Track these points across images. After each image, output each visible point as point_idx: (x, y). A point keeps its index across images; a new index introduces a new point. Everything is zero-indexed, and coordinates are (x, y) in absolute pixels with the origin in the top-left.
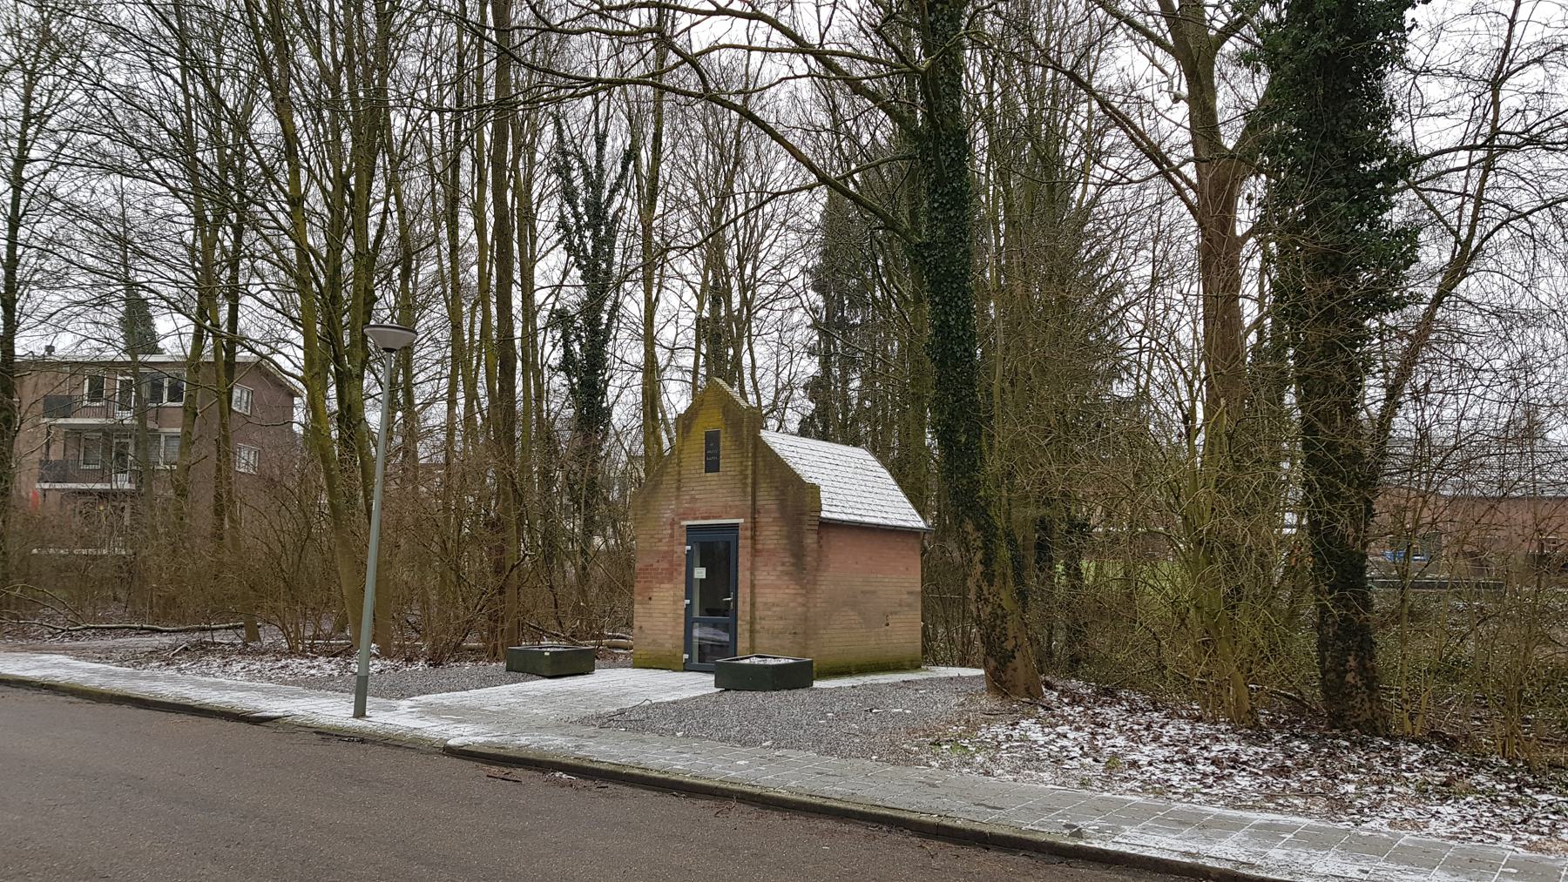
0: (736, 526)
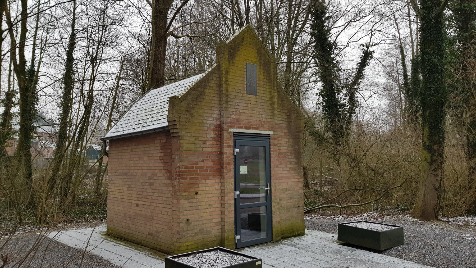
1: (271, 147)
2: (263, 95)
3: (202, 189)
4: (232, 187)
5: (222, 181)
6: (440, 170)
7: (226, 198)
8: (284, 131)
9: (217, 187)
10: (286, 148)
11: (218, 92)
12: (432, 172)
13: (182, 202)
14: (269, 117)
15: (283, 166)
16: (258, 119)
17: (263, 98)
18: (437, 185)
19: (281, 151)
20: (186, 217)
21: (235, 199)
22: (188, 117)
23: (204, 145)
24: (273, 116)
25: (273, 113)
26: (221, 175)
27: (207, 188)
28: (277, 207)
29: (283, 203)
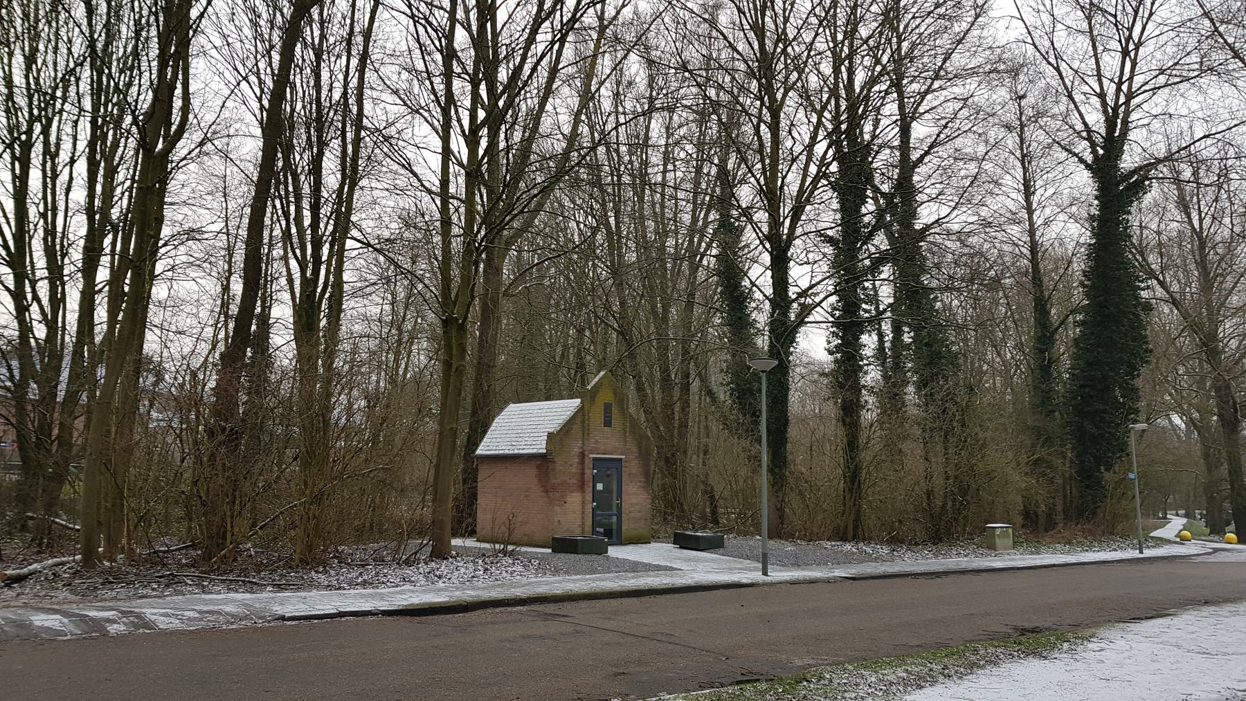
0: (621, 459)
3: (568, 500)
9: (580, 499)
18: (779, 506)
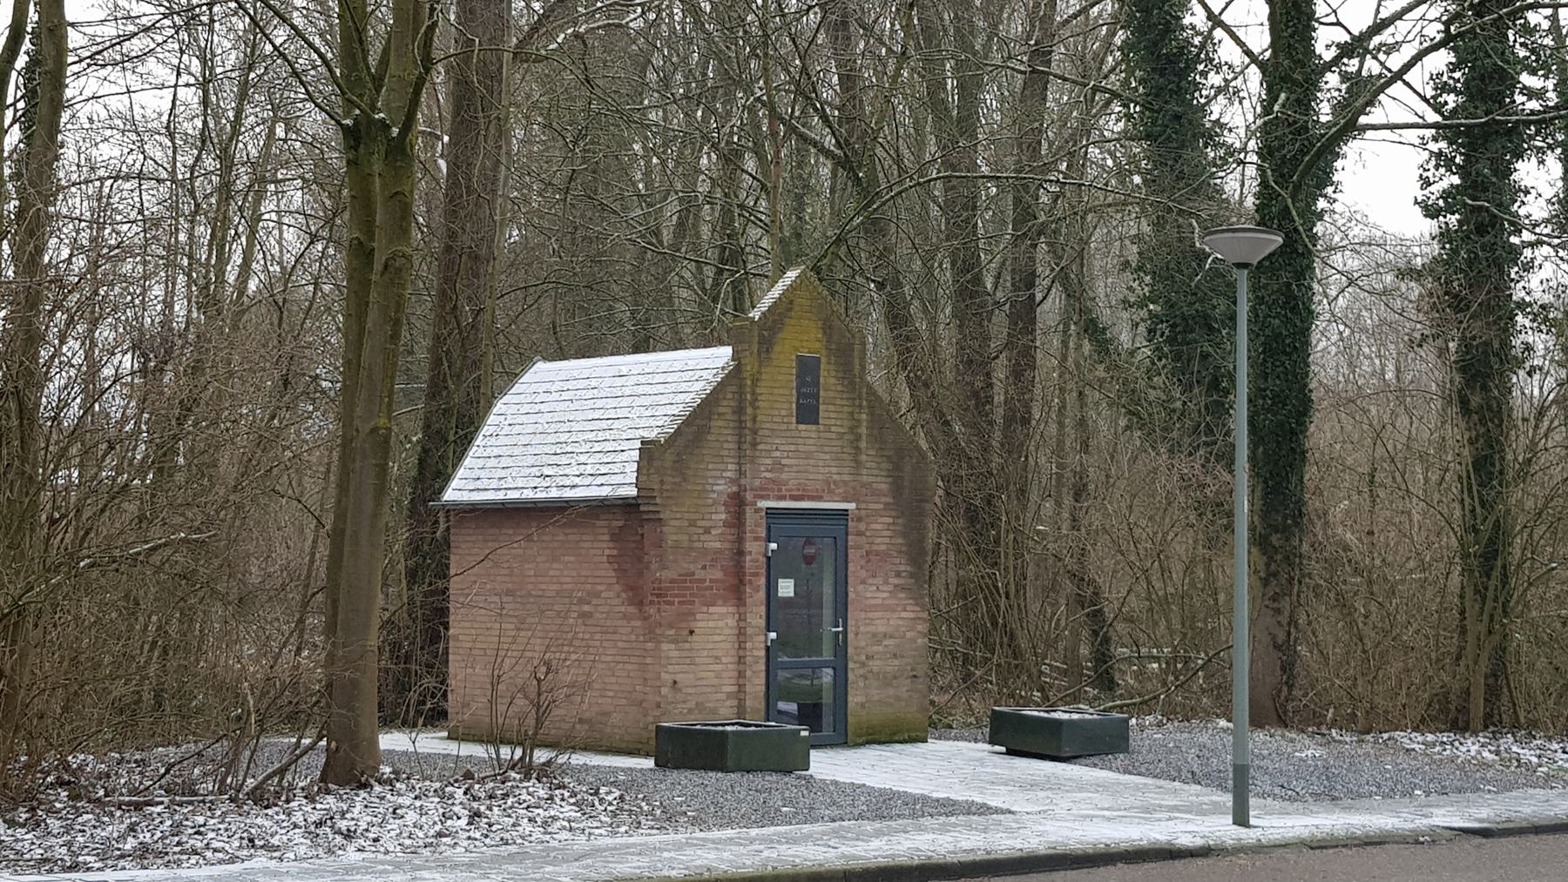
1: (850, 537)
2: (833, 422)
3: (700, 625)
4: (762, 623)
5: (742, 610)
6: (1287, 598)
7: (749, 645)
8: (883, 499)
9: (732, 622)
10: (887, 540)
11: (737, 425)
12: (1267, 603)
13: (665, 646)
14: (846, 470)
15: (879, 581)
16: (820, 477)
17: (833, 429)
18: (1281, 636)
19: (875, 548)
20: (673, 676)
21: (768, 649)
22: (677, 480)
23: (706, 537)
24: (857, 468)
25: (856, 461)
26: (739, 599)
27: (711, 624)
28: (861, 672)
29: (875, 665)
